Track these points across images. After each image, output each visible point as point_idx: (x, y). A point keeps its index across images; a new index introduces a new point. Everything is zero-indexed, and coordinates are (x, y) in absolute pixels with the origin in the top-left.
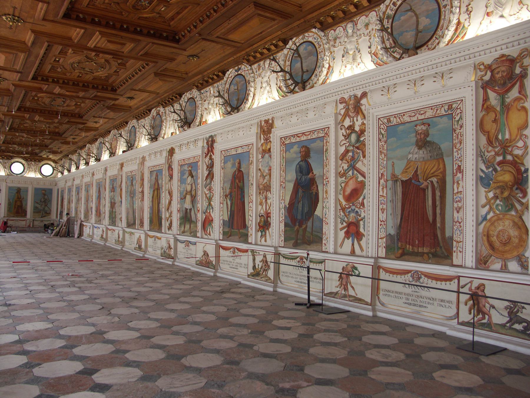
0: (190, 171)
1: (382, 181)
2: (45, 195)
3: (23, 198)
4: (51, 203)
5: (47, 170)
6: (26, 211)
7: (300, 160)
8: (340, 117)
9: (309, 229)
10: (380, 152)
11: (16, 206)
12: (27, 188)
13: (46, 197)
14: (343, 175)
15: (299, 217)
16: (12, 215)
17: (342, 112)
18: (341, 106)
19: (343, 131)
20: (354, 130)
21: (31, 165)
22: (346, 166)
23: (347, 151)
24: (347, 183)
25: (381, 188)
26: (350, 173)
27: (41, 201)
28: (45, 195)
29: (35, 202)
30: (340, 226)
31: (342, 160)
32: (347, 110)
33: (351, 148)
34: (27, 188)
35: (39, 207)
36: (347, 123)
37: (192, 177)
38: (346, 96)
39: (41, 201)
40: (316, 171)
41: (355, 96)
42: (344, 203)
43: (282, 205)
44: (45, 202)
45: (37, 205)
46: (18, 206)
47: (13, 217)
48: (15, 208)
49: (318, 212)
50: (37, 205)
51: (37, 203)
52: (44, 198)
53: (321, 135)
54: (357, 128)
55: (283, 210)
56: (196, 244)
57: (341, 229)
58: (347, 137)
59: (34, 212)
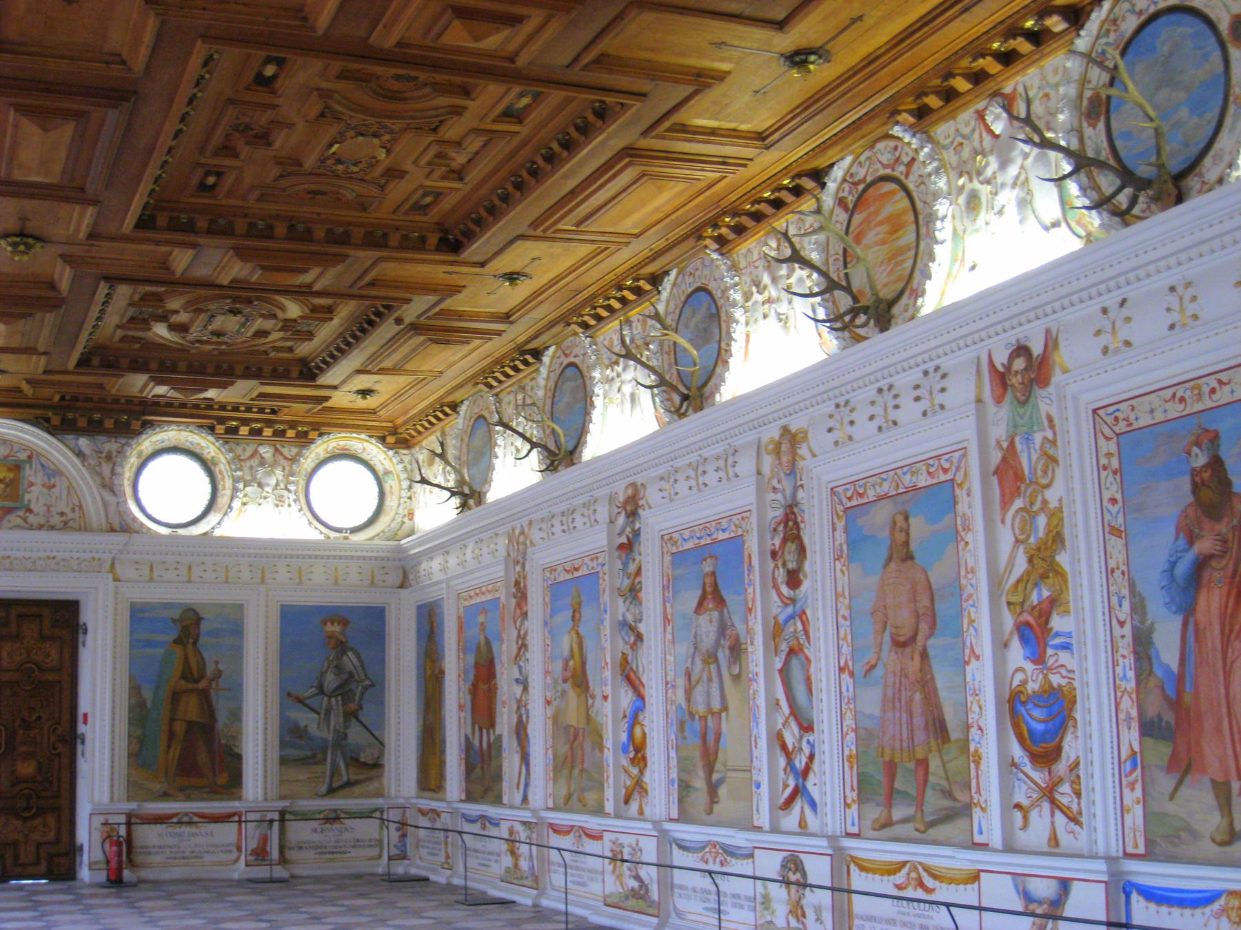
2: (341, 647)
3: (218, 674)
4: (380, 702)
6: (239, 757)
11: (179, 727)
12: (240, 608)
13: (350, 660)
16: (157, 787)
21: (255, 462)
27: (321, 690)
28: (341, 647)
29: (290, 697)
34: (240, 608)
35: (313, 729)
39: (321, 690)
44: (344, 690)
45: (305, 718)
46: (190, 724)
47: (165, 796)
48: (171, 735)
50: (305, 718)
51: (300, 701)
52: (339, 669)
56: (751, 856)
59: (283, 761)
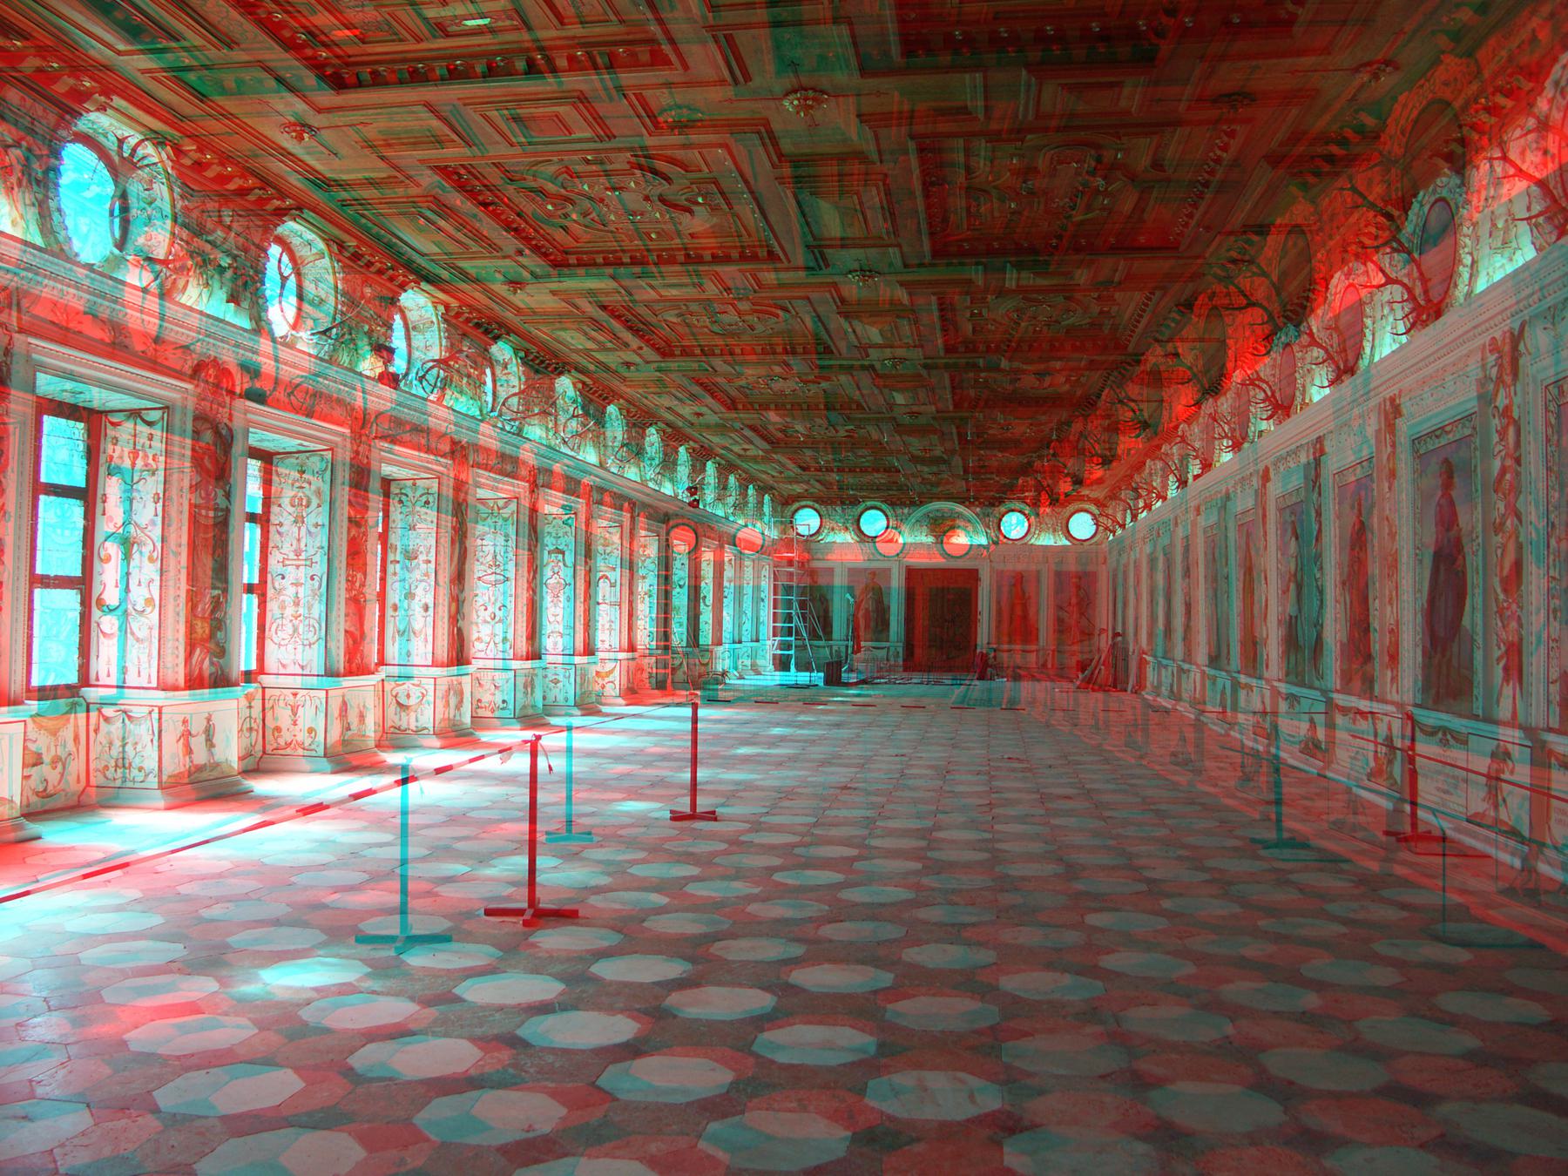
0: (1293, 522)
1: (1553, 542)
5: (1082, 525)
7: (1439, 493)
8: (1491, 387)
9: (1455, 662)
10: (1549, 469)
14: (1499, 528)
15: (1441, 633)
17: (1494, 371)
18: (1492, 359)
19: (1496, 421)
20: (1511, 417)
22: (1501, 506)
23: (1503, 470)
24: (1504, 547)
25: (1552, 557)
26: (1509, 523)
30: (1497, 653)
31: (1496, 491)
32: (1501, 366)
33: (1509, 462)
36: (1501, 401)
37: (1297, 539)
38: (1498, 335)
40: (1463, 519)
41: (1512, 334)
42: (1502, 597)
43: (1419, 603)
49: (1466, 621)
53: (1467, 432)
54: (1515, 415)
55: (1419, 616)
57: (1499, 660)
58: (1502, 434)
